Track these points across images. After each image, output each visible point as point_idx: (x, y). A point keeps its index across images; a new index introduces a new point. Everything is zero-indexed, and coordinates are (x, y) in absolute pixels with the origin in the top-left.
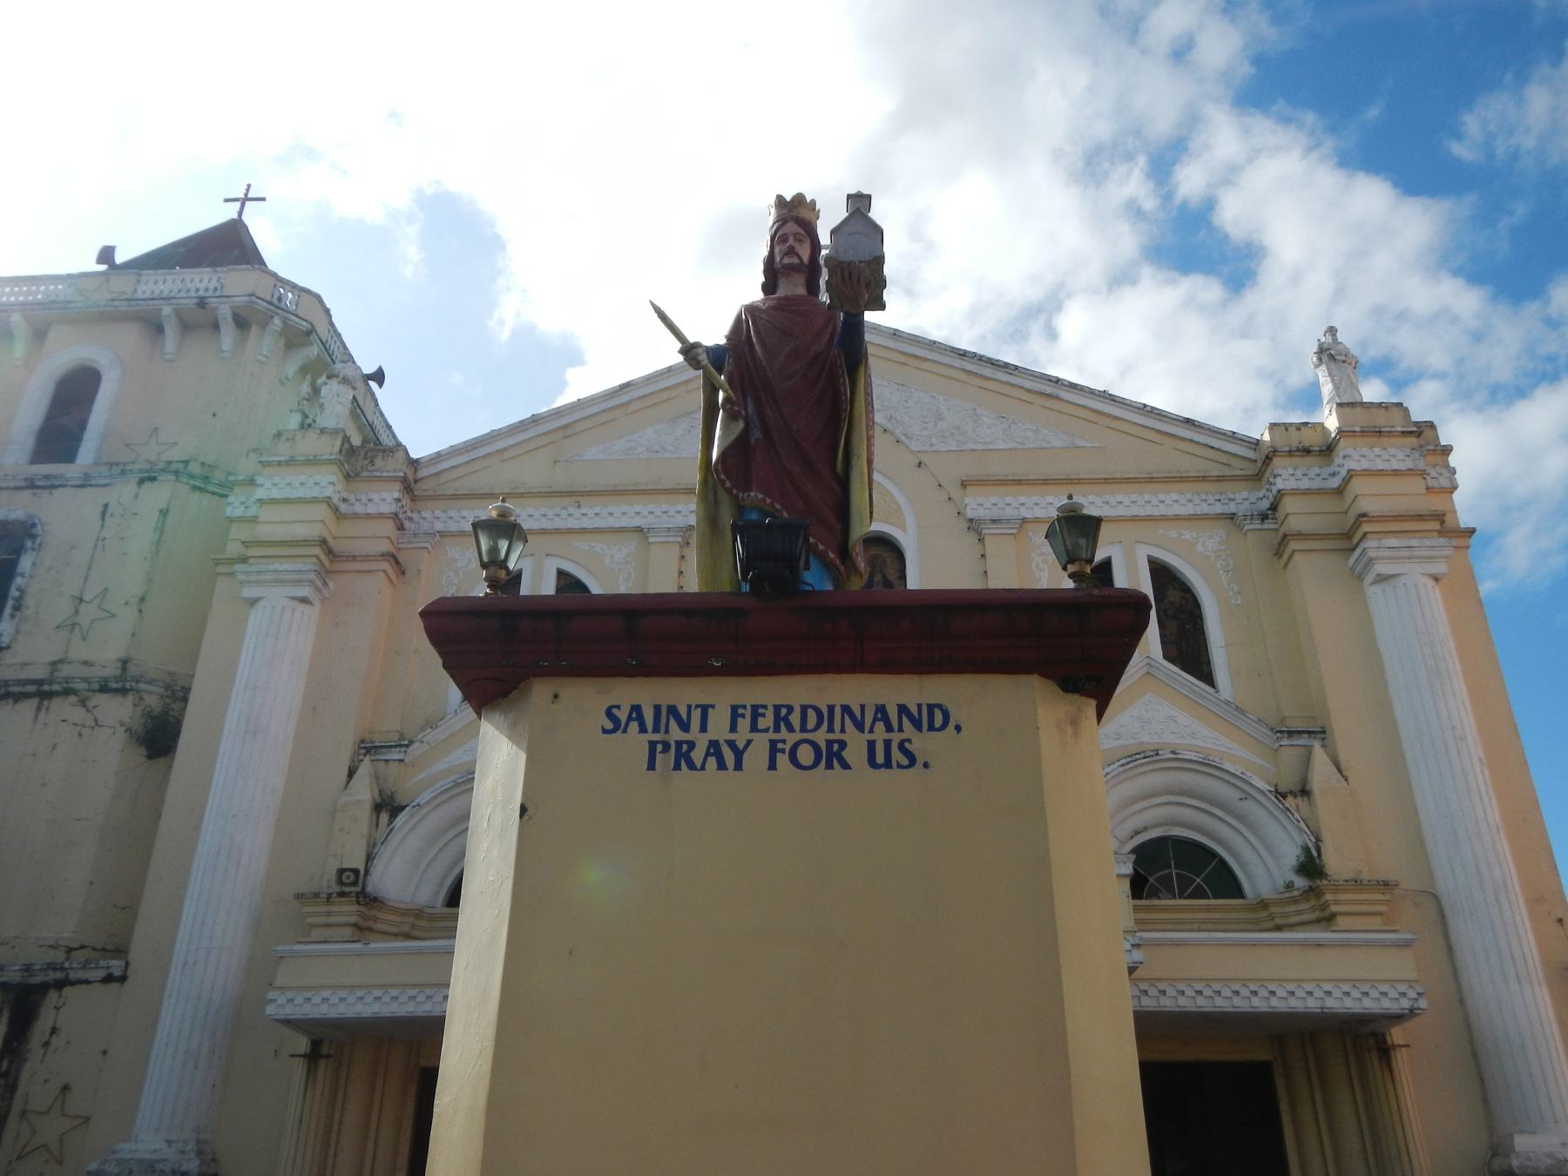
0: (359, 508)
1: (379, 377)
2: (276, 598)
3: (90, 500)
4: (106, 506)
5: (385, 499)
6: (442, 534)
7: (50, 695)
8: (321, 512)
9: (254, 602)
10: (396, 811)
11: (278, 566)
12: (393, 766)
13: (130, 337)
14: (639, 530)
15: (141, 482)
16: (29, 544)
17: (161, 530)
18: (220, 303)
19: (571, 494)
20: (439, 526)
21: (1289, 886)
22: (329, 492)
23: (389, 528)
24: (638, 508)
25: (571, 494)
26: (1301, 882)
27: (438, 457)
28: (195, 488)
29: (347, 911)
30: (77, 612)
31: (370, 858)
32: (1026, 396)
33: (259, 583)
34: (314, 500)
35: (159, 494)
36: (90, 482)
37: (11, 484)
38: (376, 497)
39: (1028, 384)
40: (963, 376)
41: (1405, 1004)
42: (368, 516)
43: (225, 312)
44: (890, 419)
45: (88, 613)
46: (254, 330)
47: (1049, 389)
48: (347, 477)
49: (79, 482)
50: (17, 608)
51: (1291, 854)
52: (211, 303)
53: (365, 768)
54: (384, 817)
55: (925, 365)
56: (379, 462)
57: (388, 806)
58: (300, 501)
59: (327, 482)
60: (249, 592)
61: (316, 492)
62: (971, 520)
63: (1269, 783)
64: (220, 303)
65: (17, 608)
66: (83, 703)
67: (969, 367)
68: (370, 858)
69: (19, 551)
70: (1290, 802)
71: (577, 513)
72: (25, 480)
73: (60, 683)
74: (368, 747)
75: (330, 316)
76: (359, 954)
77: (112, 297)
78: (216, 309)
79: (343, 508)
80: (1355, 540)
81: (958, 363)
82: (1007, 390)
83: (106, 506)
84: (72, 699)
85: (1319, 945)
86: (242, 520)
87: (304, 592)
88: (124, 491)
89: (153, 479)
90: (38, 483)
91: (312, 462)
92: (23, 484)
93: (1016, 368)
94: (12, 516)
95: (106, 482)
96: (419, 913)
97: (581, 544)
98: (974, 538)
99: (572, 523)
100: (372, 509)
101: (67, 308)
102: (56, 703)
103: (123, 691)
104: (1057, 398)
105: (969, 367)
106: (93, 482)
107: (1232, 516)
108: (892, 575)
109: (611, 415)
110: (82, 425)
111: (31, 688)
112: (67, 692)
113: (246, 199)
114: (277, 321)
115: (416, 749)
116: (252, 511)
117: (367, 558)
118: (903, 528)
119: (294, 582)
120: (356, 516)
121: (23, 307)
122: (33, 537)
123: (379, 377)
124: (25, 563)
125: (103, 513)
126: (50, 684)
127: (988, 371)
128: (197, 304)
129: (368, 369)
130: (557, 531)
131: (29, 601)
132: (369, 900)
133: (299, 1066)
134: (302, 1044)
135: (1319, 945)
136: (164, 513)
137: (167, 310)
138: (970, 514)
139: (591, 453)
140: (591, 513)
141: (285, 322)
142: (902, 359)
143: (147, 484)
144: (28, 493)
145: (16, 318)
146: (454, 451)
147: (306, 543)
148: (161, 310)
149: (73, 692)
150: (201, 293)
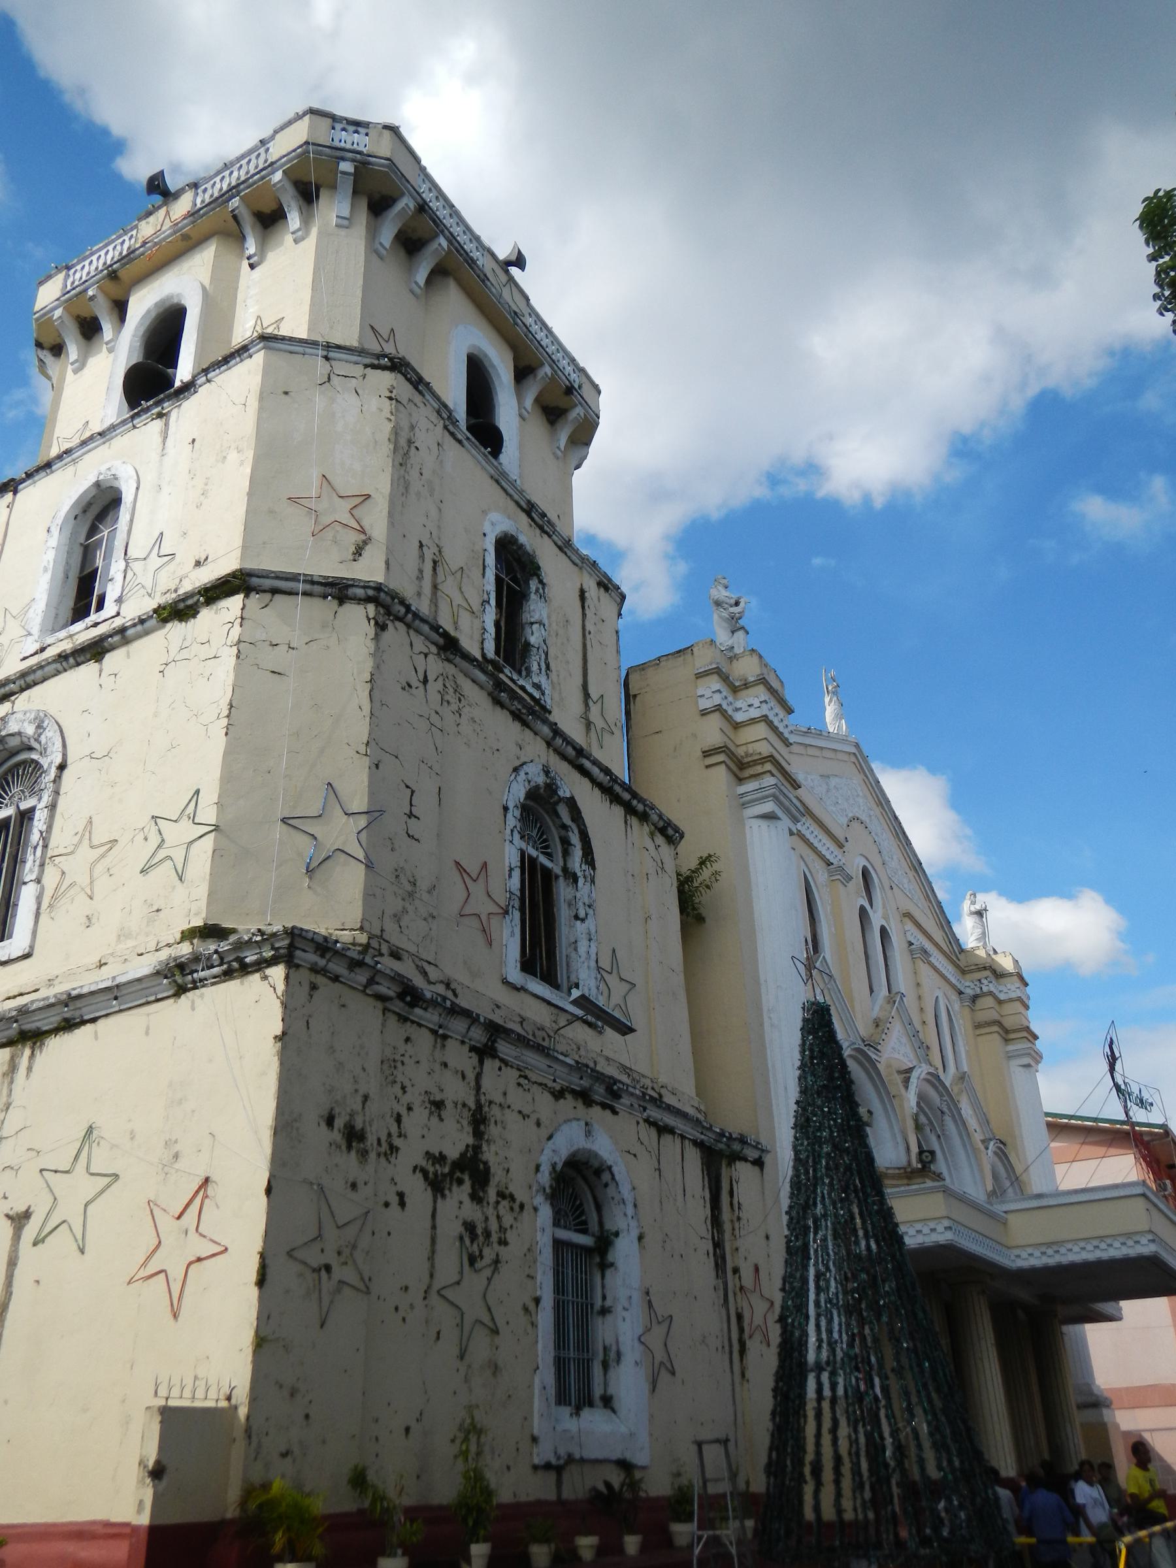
18: (580, 404)
36: (566, 550)
37: (516, 497)
49: (560, 543)
52: (576, 397)
62: (911, 944)
64: (580, 404)
66: (652, 835)
72: (529, 502)
73: (645, 805)
77: (517, 311)
78: (576, 405)
80: (1012, 1036)
89: (607, 589)
90: (533, 515)
92: (525, 506)
95: (577, 561)
101: (483, 281)
106: (569, 553)
107: (961, 993)
111: (626, 796)
121: (452, 239)
126: (639, 802)
128: (567, 387)
148: (543, 364)
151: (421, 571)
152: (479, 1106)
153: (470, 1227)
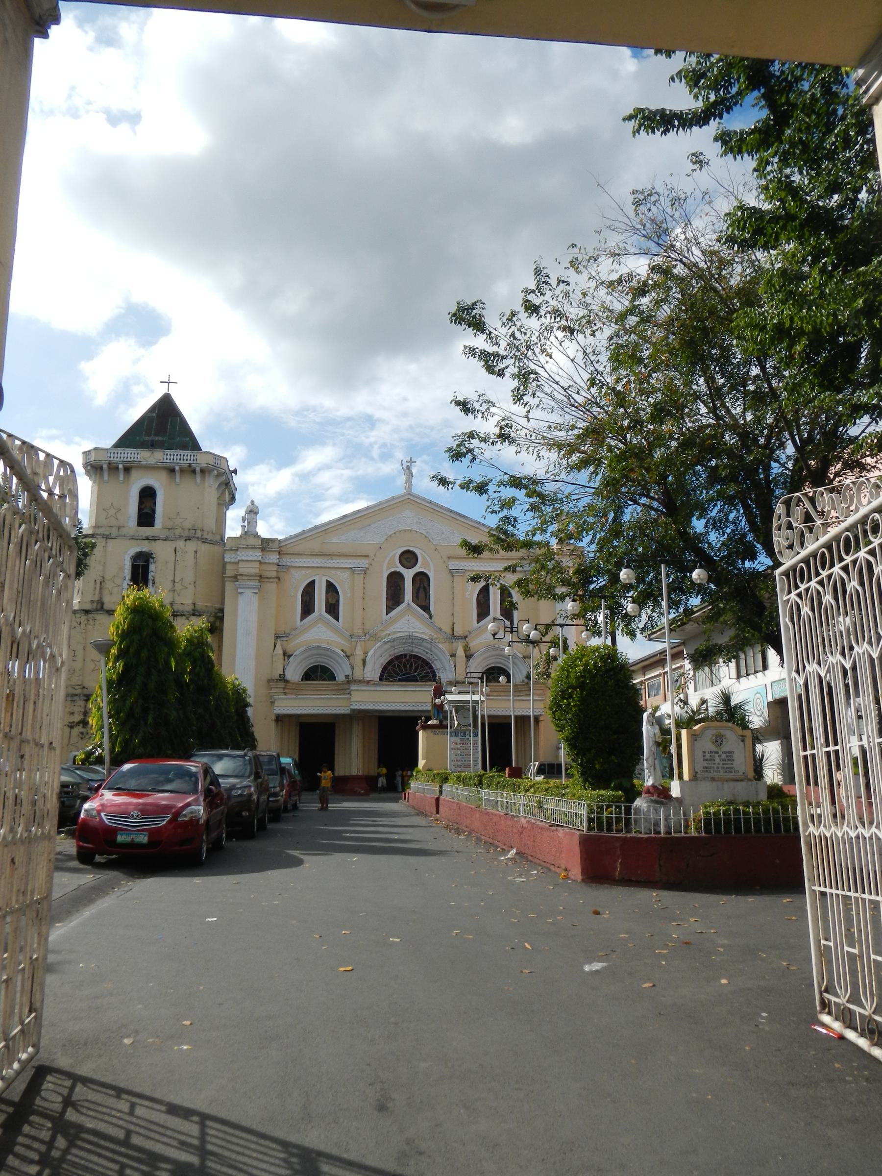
0: (266, 561)
1: (235, 472)
2: (249, 593)
3: (169, 546)
4: (176, 548)
5: (273, 558)
6: (292, 567)
7: (177, 616)
8: (257, 565)
9: (241, 593)
10: (289, 656)
11: (248, 583)
12: (285, 642)
13: (164, 475)
14: (351, 568)
15: (186, 540)
16: (151, 560)
17: (196, 558)
19: (329, 555)
20: (288, 564)
21: (523, 681)
22: (260, 558)
23: (275, 567)
24: (350, 561)
25: (329, 555)
26: (526, 680)
27: (286, 539)
28: (203, 542)
29: (282, 685)
30: (174, 586)
31: (284, 669)
32: (469, 527)
33: (244, 588)
34: (255, 561)
35: (192, 546)
38: (272, 558)
39: (470, 523)
40: (451, 519)
41: (539, 713)
42: (269, 563)
43: (198, 469)
44: (427, 533)
45: (178, 587)
46: (207, 474)
47: (476, 525)
48: (262, 550)
50: (154, 583)
51: (525, 673)
53: (279, 643)
54: (286, 658)
55: (439, 514)
56: (271, 545)
57: (287, 655)
58: (251, 561)
59: (257, 555)
60: (240, 590)
61: (256, 559)
63: (522, 654)
65: (154, 583)
66: (188, 618)
67: (453, 515)
68: (284, 669)
69: (147, 562)
70: (526, 660)
71: (332, 562)
74: (277, 637)
75: (227, 461)
76: (295, 699)
79: (262, 560)
81: (449, 514)
82: (465, 525)
83: (176, 548)
84: (184, 617)
85: (523, 700)
86: (229, 562)
87: (256, 591)
88: (180, 544)
89: (190, 539)
91: (253, 548)
93: (467, 517)
94: (143, 550)
96: (297, 684)
97: (333, 572)
98: (449, 576)
99: (330, 565)
100: (271, 561)
102: (179, 618)
103: (200, 615)
104: (478, 528)
105: (453, 515)
108: (426, 585)
109: (339, 527)
110: (154, 511)
112: (182, 615)
113: (169, 383)
114: (215, 472)
115: (290, 637)
116: (233, 560)
117: (271, 578)
118: (430, 570)
119: (254, 588)
120: (266, 563)
122: (153, 558)
123: (235, 472)
124: (152, 567)
125: (175, 550)
127: (458, 518)
129: (232, 469)
130: (326, 568)
131: (156, 580)
132: (287, 681)
133: (273, 724)
134: (274, 718)
135: (523, 700)
136: (196, 552)
137: (177, 468)
138: (450, 568)
139: (335, 540)
140: (336, 562)
141: (217, 471)
142: (432, 511)
143: (188, 541)
144: (146, 541)
145: (121, 466)
146: (291, 537)
147: (256, 576)
149: (184, 615)
150: (189, 462)
151: (95, 588)
152: (86, 711)
153: (82, 733)
